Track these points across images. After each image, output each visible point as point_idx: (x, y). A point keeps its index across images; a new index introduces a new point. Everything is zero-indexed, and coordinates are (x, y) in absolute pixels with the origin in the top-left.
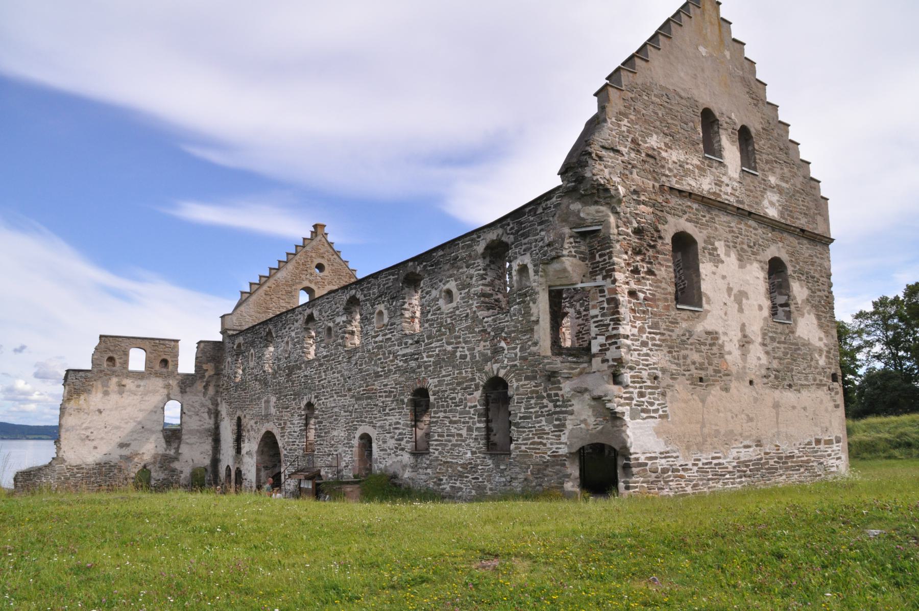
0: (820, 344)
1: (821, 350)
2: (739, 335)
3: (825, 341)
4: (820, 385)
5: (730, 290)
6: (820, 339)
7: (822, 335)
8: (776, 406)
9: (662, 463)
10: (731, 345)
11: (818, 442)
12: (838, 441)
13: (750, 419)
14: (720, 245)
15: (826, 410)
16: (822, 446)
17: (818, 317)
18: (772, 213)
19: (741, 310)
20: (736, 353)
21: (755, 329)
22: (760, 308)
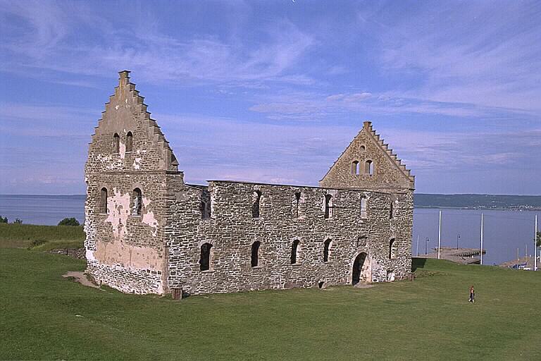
0: (155, 226)
1: (155, 229)
2: (119, 223)
3: (157, 224)
4: (152, 245)
5: (116, 206)
6: (155, 224)
7: (156, 221)
8: (130, 252)
9: (94, 264)
10: (115, 226)
11: (149, 271)
12: (159, 273)
13: (120, 256)
14: (115, 189)
15: (154, 258)
16: (150, 274)
17: (155, 213)
18: (137, 167)
19: (120, 213)
20: (117, 230)
21: (124, 222)
22: (127, 212)
